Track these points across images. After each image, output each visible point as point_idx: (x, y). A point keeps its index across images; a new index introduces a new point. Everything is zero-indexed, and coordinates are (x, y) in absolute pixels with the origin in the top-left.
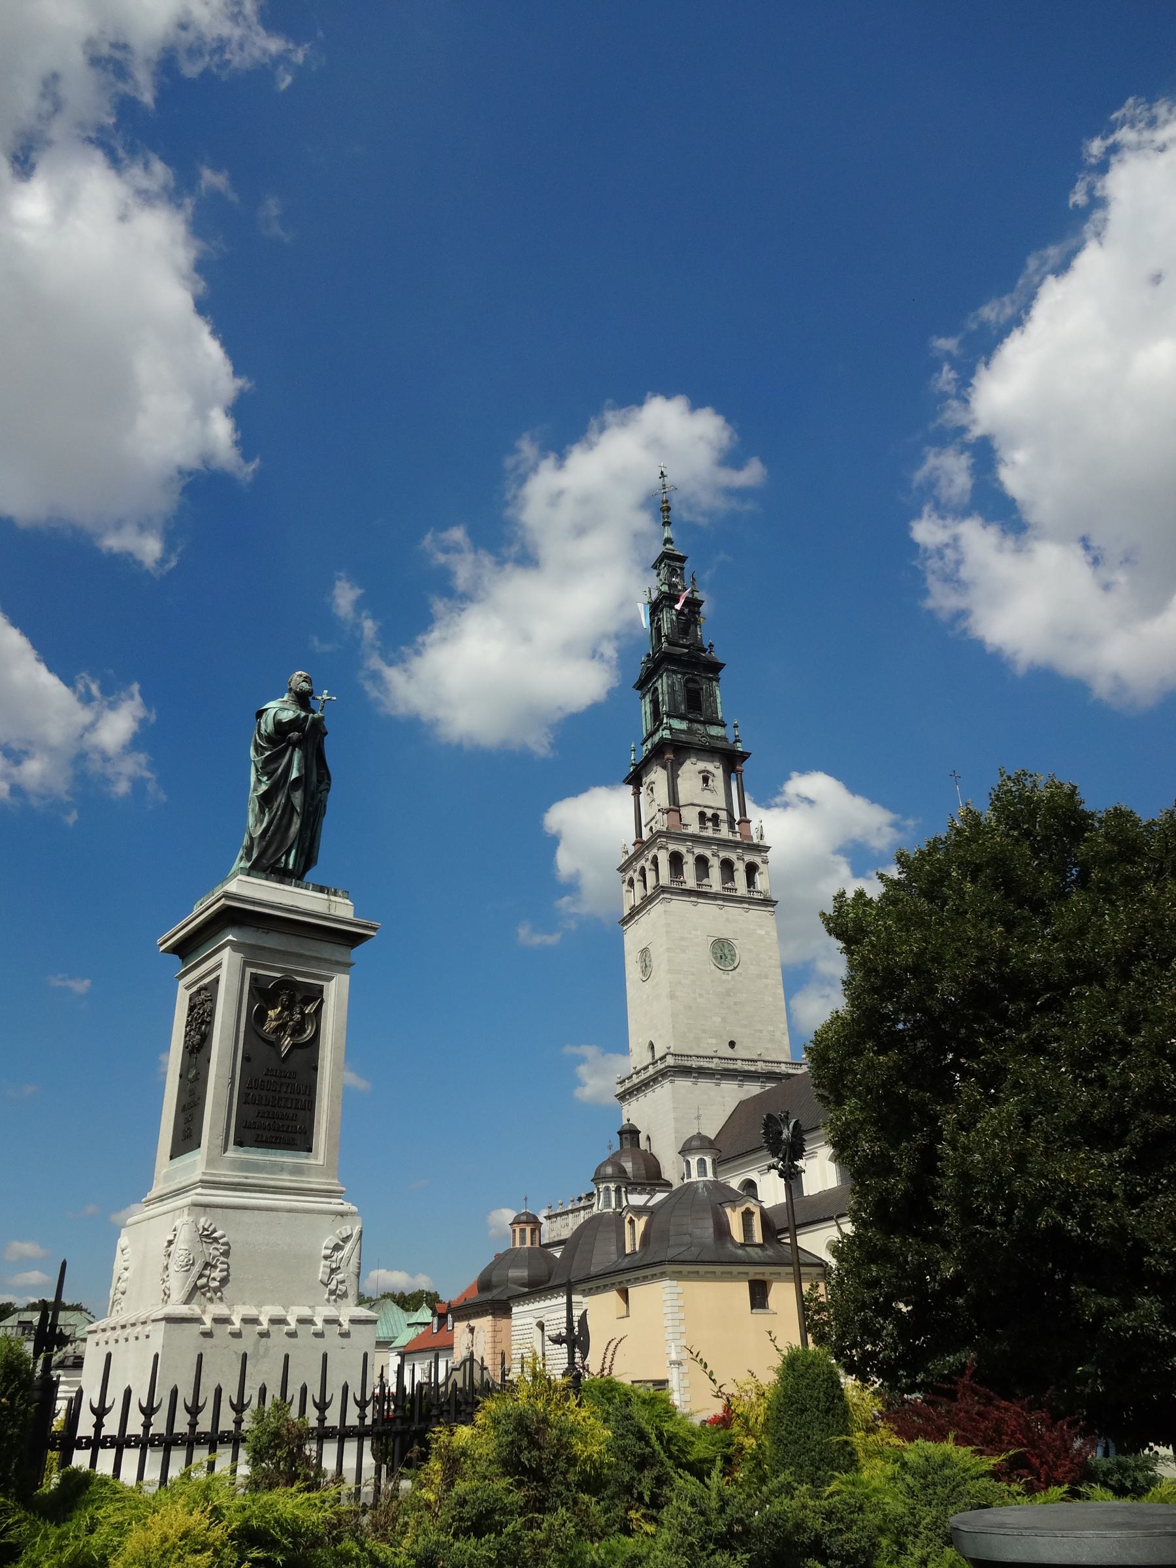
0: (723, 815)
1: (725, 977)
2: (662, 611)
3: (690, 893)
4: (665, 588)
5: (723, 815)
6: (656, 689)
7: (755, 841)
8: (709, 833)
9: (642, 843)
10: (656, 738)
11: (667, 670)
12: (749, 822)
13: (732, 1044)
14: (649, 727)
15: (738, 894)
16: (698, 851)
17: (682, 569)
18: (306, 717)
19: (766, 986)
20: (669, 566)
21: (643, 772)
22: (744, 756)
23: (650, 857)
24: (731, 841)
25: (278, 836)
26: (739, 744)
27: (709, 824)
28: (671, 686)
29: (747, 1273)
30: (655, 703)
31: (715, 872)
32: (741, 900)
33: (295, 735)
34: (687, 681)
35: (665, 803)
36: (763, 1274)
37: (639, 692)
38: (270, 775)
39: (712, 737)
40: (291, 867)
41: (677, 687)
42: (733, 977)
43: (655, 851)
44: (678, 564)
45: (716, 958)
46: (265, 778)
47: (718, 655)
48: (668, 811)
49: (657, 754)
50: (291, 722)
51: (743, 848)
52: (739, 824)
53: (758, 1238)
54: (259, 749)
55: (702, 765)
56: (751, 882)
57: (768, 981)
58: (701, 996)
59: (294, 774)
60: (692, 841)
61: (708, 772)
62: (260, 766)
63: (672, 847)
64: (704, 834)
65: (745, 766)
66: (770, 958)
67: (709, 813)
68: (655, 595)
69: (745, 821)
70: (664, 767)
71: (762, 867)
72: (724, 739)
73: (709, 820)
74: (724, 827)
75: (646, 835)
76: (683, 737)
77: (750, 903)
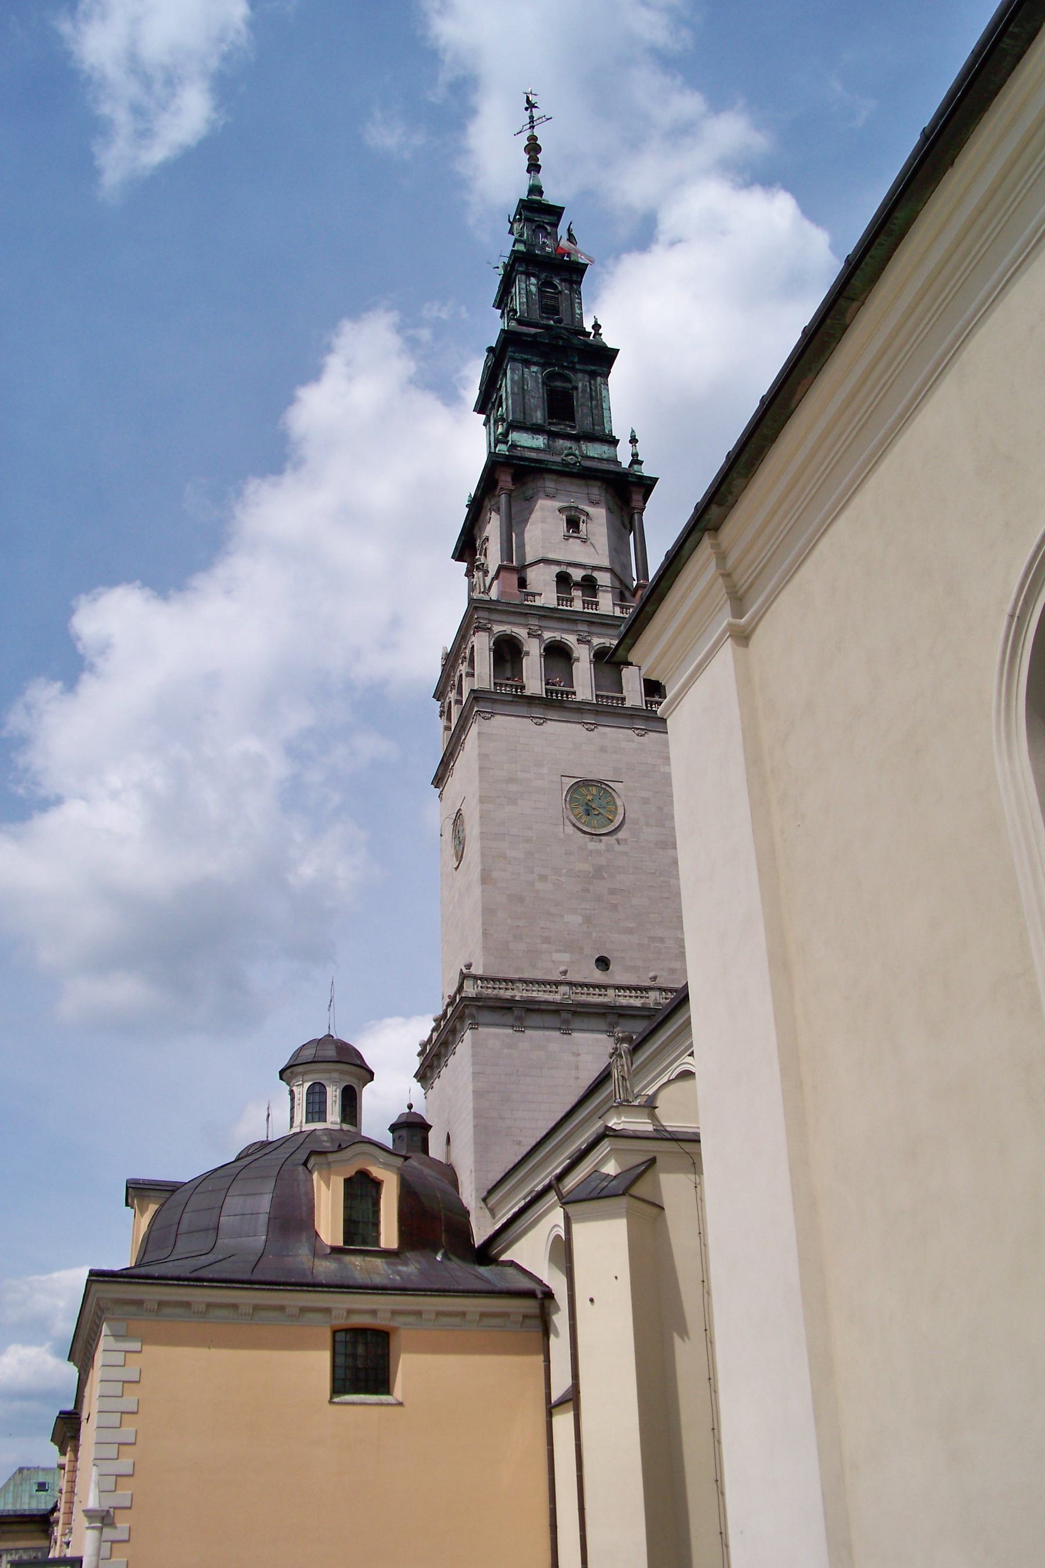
1: (593, 845)
5: (604, 579)
8: (578, 606)
11: (513, 359)
13: (603, 963)
22: (647, 485)
27: (577, 593)
28: (521, 385)
29: (327, 1311)
36: (374, 1312)
41: (530, 385)
42: (609, 849)
44: (547, 219)
47: (609, 339)
53: (389, 1236)
58: (543, 878)
67: (577, 575)
73: (577, 585)
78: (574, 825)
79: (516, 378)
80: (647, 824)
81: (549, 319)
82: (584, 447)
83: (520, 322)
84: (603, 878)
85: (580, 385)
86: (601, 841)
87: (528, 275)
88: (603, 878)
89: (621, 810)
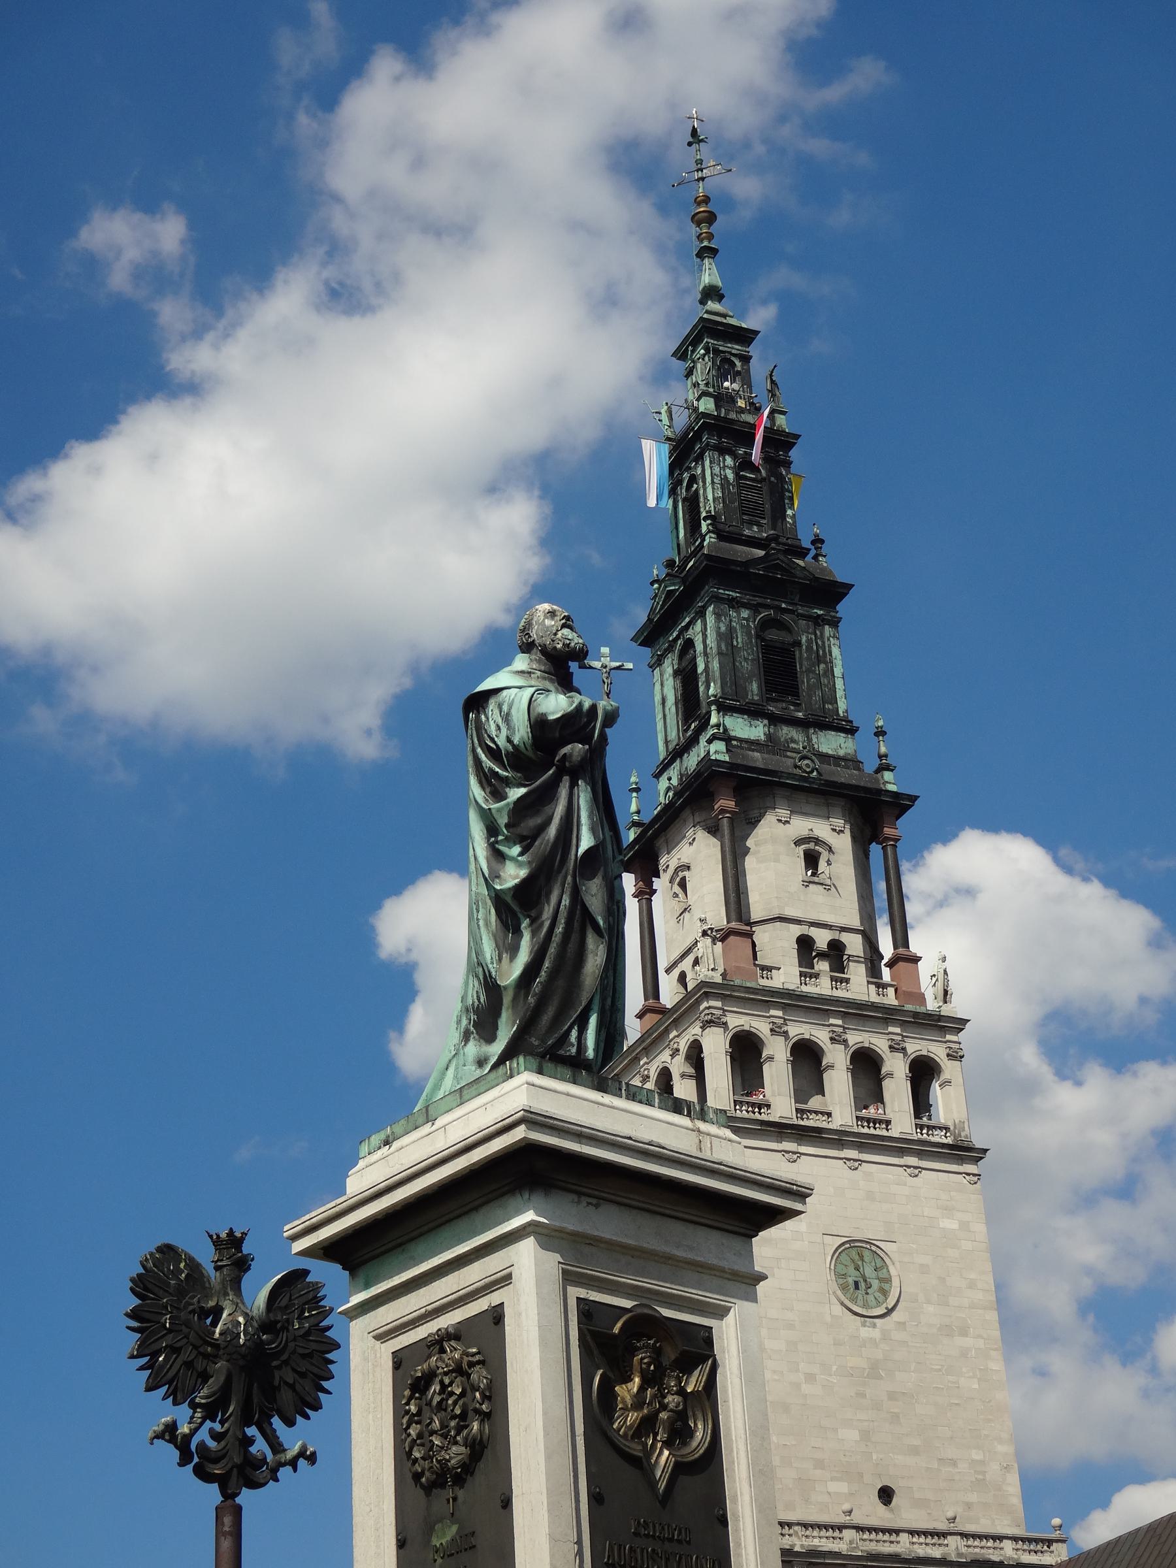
0: (854, 944)
1: (866, 1332)
2: (700, 458)
3: (780, 1130)
4: (707, 405)
5: (854, 944)
6: (690, 643)
7: (932, 1005)
8: (823, 987)
9: (662, 1011)
10: (691, 761)
11: (716, 599)
12: (915, 960)
13: (886, 1495)
14: (673, 735)
15: (895, 1132)
16: (798, 1030)
17: (746, 359)
18: (594, 708)
19: (964, 1353)
20: (717, 352)
21: (660, 842)
22: (901, 804)
23: (683, 1044)
24: (874, 1006)
25: (561, 983)
26: (888, 776)
27: (823, 966)
28: (726, 637)
30: (687, 678)
31: (839, 1078)
32: (899, 1147)
33: (575, 750)
34: (765, 625)
35: (718, 917)
37: (647, 651)
38: (527, 842)
39: (824, 757)
40: (590, 1053)
41: (740, 640)
42: (886, 1336)
43: (695, 1030)
44: (737, 348)
45: (844, 1288)
46: (516, 850)
48: (724, 936)
49: (695, 798)
50: (568, 719)
51: (902, 1024)
52: (890, 965)
54: (494, 786)
55: (802, 825)
56: (921, 1105)
57: (968, 1342)
58: (810, 1378)
59: (586, 841)
60: (784, 1007)
61: (817, 841)
62: (502, 820)
63: (737, 1021)
64: (810, 989)
65: (905, 827)
66: (972, 1285)
67: (822, 939)
68: (682, 419)
69: (905, 959)
70: (713, 830)
71: (949, 1069)
72: (852, 762)
73: (822, 955)
74: (857, 973)
75: (669, 994)
76: (757, 758)
77: (920, 1154)
78: (842, 1304)
79: (723, 629)
80: (929, 1302)
81: (751, 523)
82: (814, 740)
83: (722, 536)
84: (880, 1378)
85: (804, 639)
86: (874, 1326)
87: (722, 451)
88: (880, 1378)
89: (895, 1282)
